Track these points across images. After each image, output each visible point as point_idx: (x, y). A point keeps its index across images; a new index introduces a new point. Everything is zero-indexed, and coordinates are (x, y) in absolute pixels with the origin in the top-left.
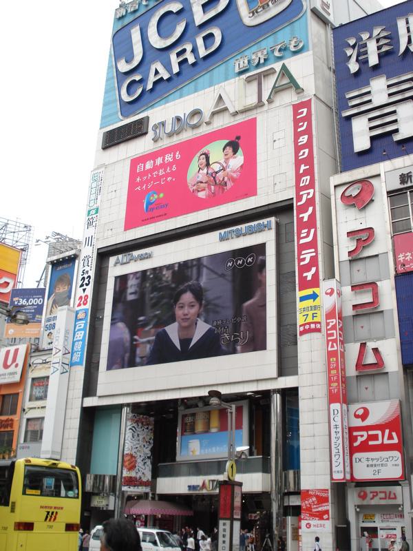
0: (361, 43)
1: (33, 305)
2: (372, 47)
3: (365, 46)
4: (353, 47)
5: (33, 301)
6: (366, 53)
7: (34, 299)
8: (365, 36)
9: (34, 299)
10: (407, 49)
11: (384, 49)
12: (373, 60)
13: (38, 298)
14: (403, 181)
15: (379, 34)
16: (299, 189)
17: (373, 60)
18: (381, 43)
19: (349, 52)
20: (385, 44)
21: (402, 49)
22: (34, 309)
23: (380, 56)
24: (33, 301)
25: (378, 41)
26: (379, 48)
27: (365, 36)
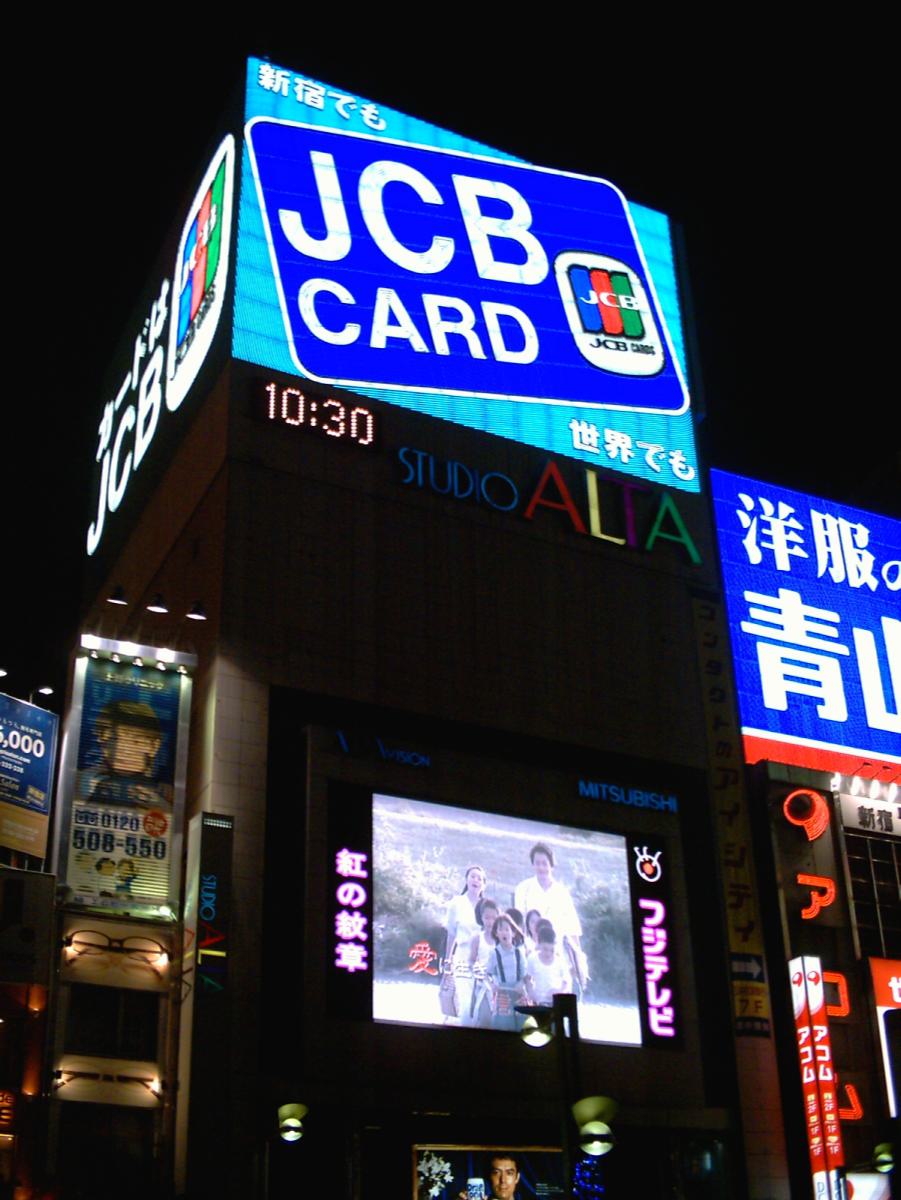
0: (763, 517)
1: (19, 751)
2: (777, 530)
5: (21, 741)
6: (769, 539)
7: (23, 733)
9: (23, 733)
11: (798, 552)
12: (783, 564)
13: (34, 737)
15: (787, 519)
17: (783, 564)
20: (799, 544)
21: (821, 573)
22: (25, 765)
23: (792, 558)
24: (21, 741)
25: (788, 530)
26: (790, 544)
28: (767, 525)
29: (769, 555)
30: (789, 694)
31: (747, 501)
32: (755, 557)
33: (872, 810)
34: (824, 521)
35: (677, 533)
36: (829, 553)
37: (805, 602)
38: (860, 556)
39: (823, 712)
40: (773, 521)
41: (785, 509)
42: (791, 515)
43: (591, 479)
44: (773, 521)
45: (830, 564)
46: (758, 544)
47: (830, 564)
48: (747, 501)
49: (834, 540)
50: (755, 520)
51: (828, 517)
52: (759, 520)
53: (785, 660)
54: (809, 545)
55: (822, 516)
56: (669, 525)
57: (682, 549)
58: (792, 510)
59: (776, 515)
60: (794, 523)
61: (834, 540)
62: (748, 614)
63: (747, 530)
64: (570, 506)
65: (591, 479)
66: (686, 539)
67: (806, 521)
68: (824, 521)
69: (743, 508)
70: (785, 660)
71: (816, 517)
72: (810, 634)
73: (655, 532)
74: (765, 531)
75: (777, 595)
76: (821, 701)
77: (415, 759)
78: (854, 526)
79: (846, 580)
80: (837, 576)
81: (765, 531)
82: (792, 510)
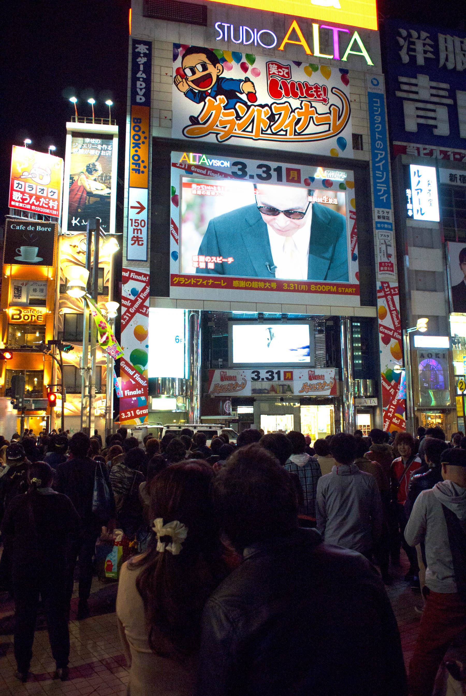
2: (419, 47)
3: (414, 43)
4: (405, 39)
6: (414, 50)
8: (414, 34)
10: (445, 65)
11: (430, 55)
12: (420, 61)
14: (451, 180)
15: (425, 40)
16: (374, 156)
17: (420, 61)
18: (425, 49)
19: (401, 41)
20: (431, 52)
23: (426, 59)
25: (424, 45)
26: (425, 52)
27: (414, 34)
28: (414, 43)
29: (413, 59)
30: (419, 125)
31: (404, 33)
32: (406, 59)
33: (456, 175)
34: (445, 39)
35: (360, 51)
36: (447, 55)
37: (431, 80)
38: (464, 55)
39: (437, 132)
40: (417, 41)
41: (424, 35)
42: (427, 37)
43: (316, 27)
44: (417, 41)
45: (447, 60)
46: (408, 53)
47: (447, 60)
48: (404, 33)
49: (450, 48)
50: (407, 42)
51: (449, 37)
52: (409, 41)
53: (417, 109)
54: (436, 52)
55: (444, 36)
56: (356, 47)
57: (363, 57)
58: (429, 35)
59: (419, 38)
60: (428, 41)
61: (450, 48)
62: (399, 87)
63: (403, 46)
64: (303, 42)
65: (316, 27)
66: (365, 53)
67: (436, 40)
68: (445, 39)
69: (401, 36)
70: (417, 109)
71: (441, 38)
72: (432, 95)
73: (348, 51)
74: (412, 47)
75: (416, 78)
76: (436, 127)
77: (222, 164)
78: (461, 40)
79: (455, 67)
80: (450, 66)
81: (412, 47)
82: (429, 35)
